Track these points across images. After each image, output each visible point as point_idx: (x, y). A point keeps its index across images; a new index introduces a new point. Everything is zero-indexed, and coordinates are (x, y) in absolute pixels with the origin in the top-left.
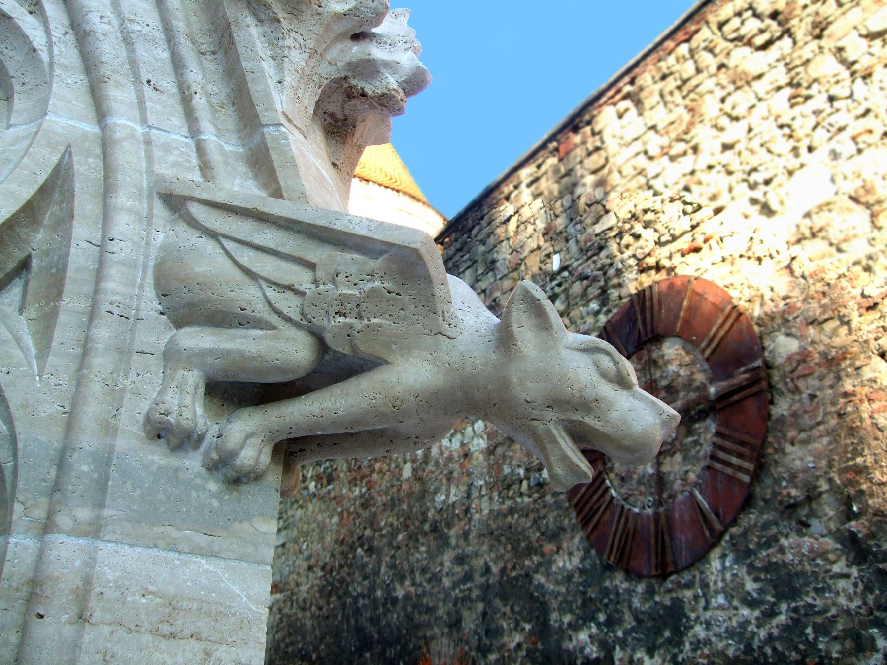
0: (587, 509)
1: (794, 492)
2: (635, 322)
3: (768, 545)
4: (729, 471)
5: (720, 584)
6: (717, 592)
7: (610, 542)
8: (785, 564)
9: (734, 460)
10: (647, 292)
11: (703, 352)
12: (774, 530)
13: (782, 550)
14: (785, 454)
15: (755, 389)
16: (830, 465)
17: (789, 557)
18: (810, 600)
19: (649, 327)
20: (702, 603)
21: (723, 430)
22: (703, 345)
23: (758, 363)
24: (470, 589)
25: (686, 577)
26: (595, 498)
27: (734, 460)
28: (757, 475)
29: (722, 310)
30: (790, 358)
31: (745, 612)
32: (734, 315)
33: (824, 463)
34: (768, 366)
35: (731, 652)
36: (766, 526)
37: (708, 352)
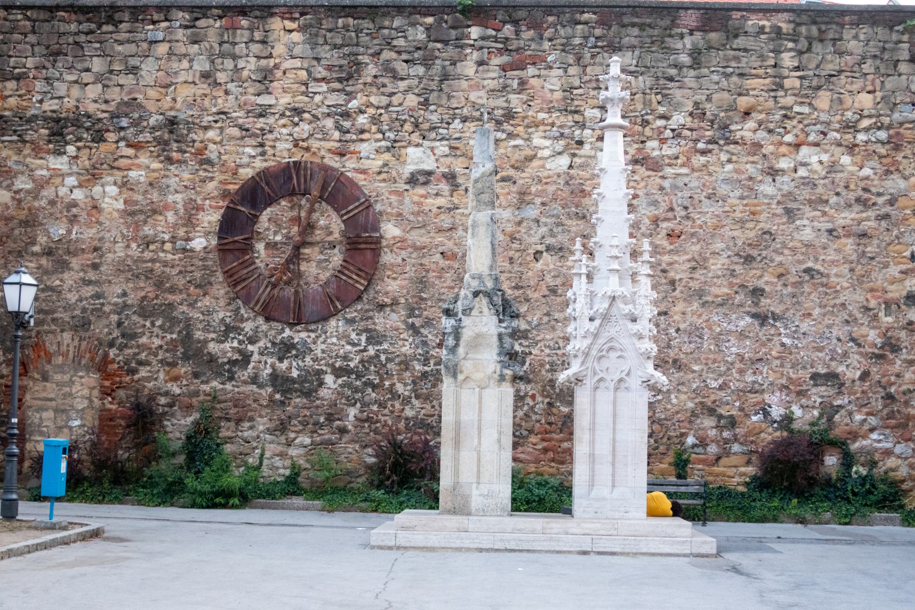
0: (236, 277)
1: (386, 300)
2: (290, 178)
3: (367, 319)
4: (350, 281)
5: (335, 334)
6: (331, 337)
7: (256, 298)
8: (375, 330)
9: (355, 277)
10: (303, 164)
11: (342, 216)
12: (371, 314)
13: (374, 324)
14: (383, 280)
15: (373, 246)
16: (408, 293)
17: (377, 328)
18: (386, 347)
19: (302, 187)
20: (321, 339)
21: (348, 259)
22: (343, 212)
23: (378, 235)
24: (103, 304)
25: (313, 327)
26: (245, 271)
27: (355, 277)
28: (366, 289)
29: (359, 200)
30: (394, 238)
31: (349, 347)
32: (366, 204)
33: (405, 291)
34: (381, 237)
35: (337, 365)
36: (367, 311)
37: (345, 217)
